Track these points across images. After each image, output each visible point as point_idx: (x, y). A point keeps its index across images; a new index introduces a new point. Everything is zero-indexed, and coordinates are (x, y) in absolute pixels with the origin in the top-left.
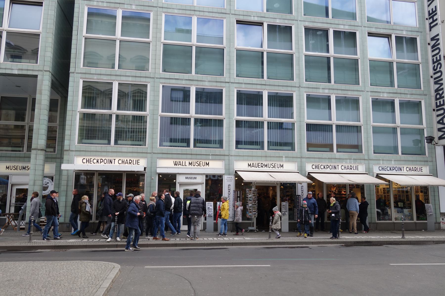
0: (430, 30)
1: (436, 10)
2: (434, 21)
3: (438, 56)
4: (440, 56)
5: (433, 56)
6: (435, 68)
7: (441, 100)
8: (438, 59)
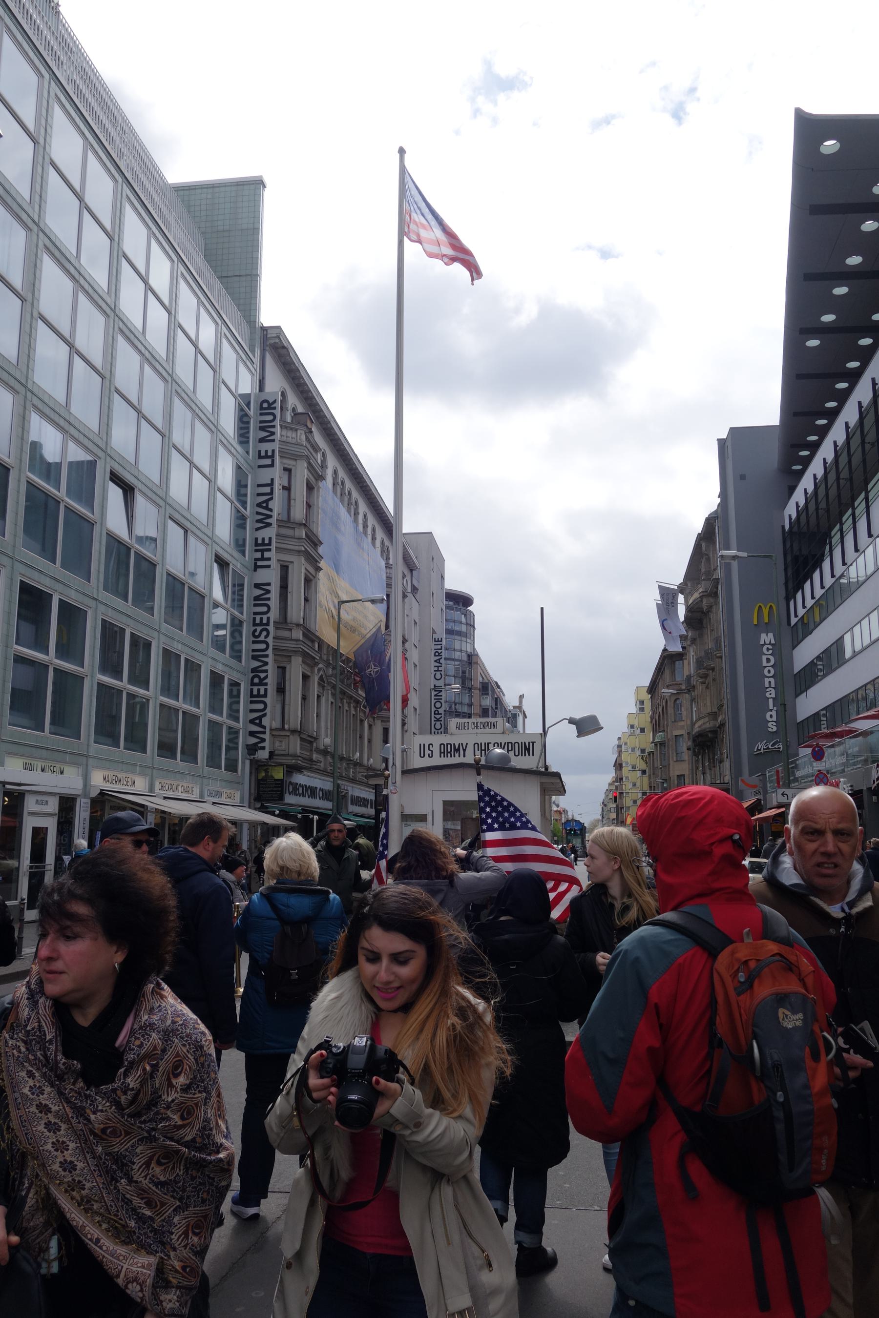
0: (255, 570)
1: (270, 544)
2: (263, 559)
3: (265, 617)
4: (268, 619)
5: (255, 613)
6: (257, 634)
7: (262, 689)
8: (265, 621)
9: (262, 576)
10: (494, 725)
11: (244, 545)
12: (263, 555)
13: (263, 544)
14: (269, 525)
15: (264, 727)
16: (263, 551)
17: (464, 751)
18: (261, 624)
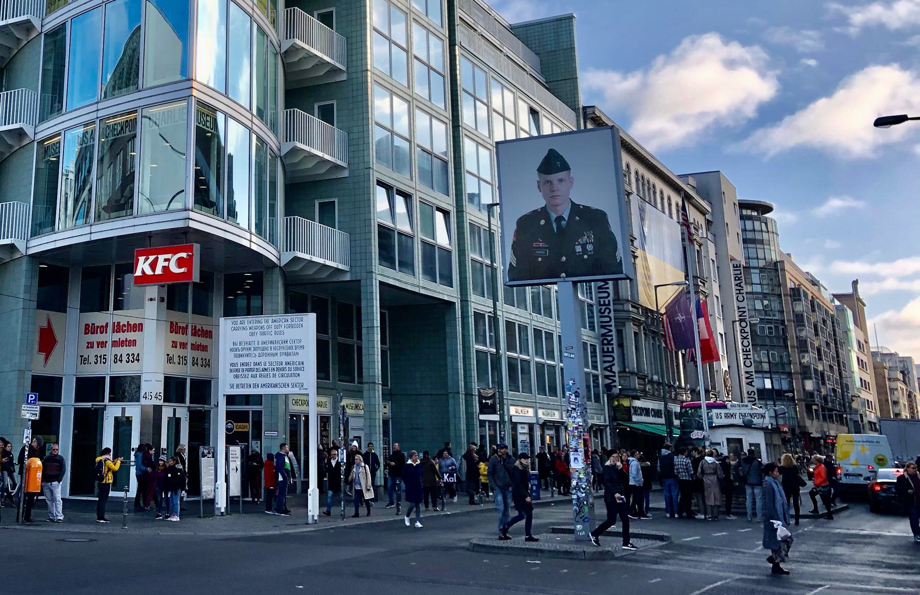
7: (610, 347)
18: (604, 305)
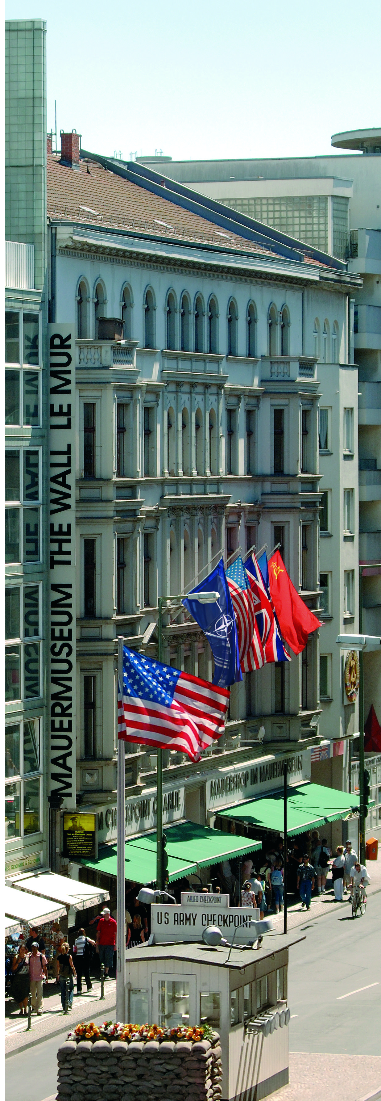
0: (52, 567)
1: (69, 533)
2: (61, 552)
3: (66, 629)
4: (70, 631)
6: (57, 650)
7: (66, 720)
8: (66, 634)
9: (62, 575)
10: (218, 900)
11: (36, 532)
12: (60, 547)
13: (61, 532)
14: (67, 507)
15: (70, 769)
16: (61, 542)
17: (194, 920)
18: (61, 638)
